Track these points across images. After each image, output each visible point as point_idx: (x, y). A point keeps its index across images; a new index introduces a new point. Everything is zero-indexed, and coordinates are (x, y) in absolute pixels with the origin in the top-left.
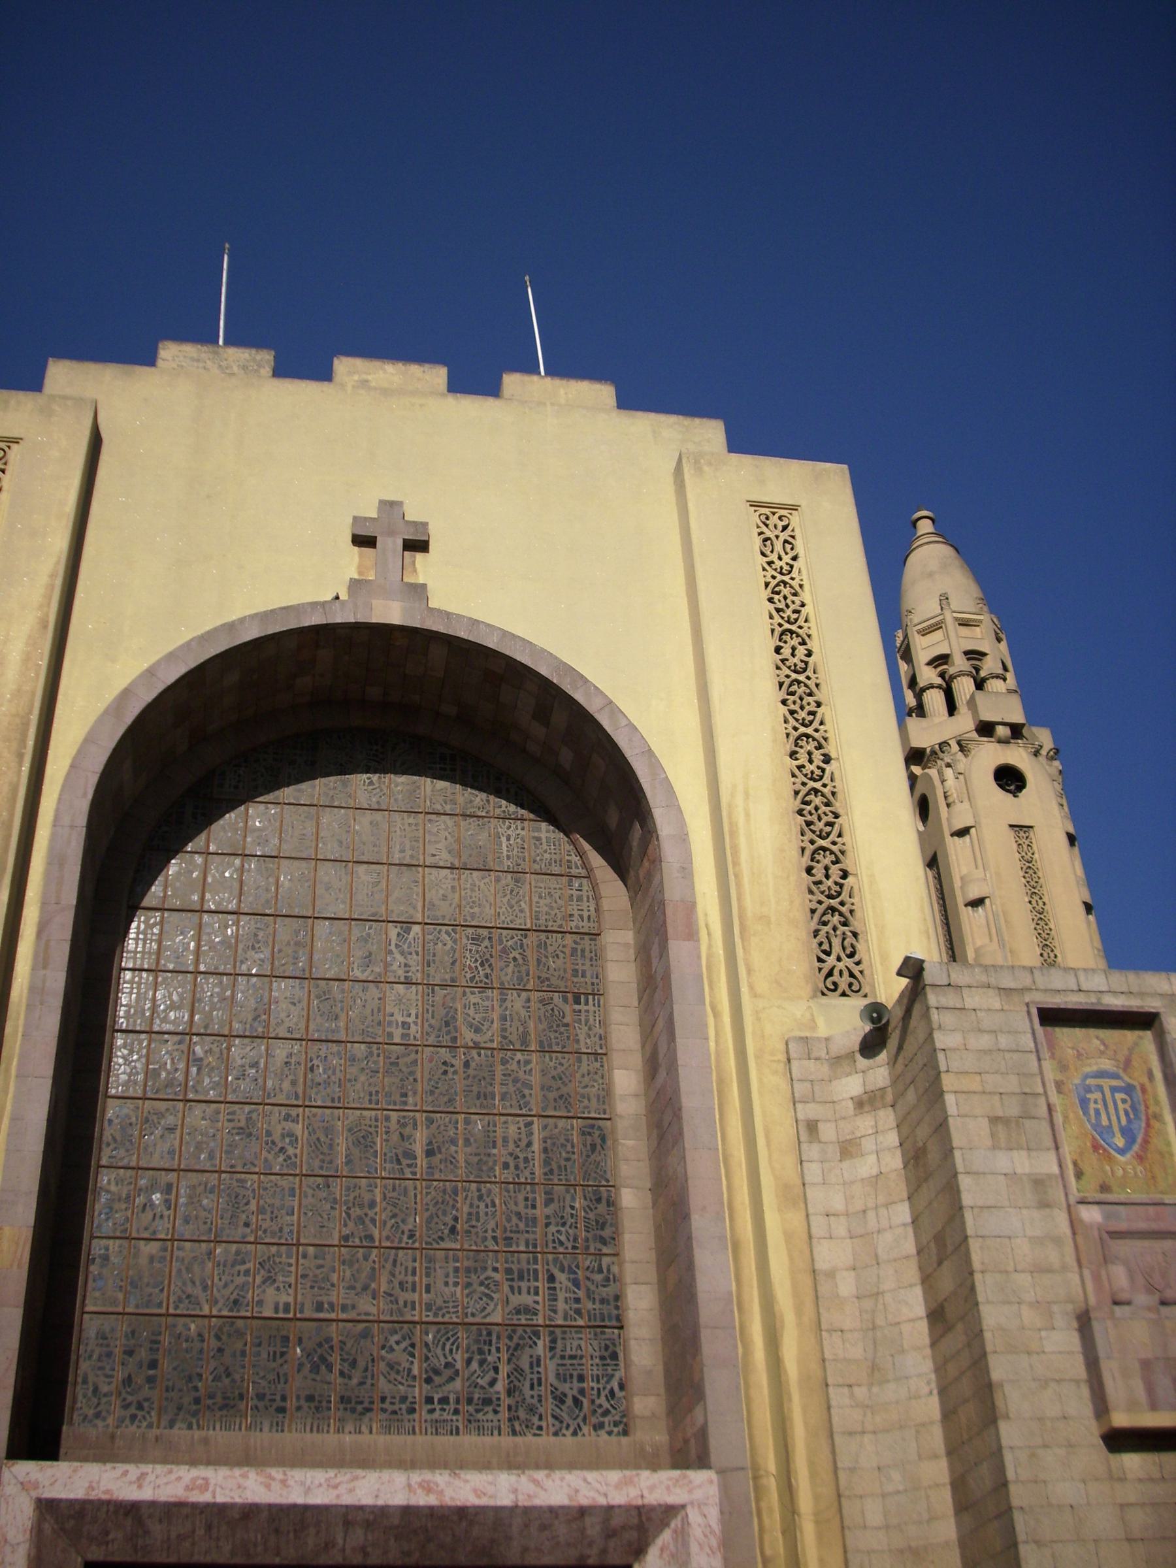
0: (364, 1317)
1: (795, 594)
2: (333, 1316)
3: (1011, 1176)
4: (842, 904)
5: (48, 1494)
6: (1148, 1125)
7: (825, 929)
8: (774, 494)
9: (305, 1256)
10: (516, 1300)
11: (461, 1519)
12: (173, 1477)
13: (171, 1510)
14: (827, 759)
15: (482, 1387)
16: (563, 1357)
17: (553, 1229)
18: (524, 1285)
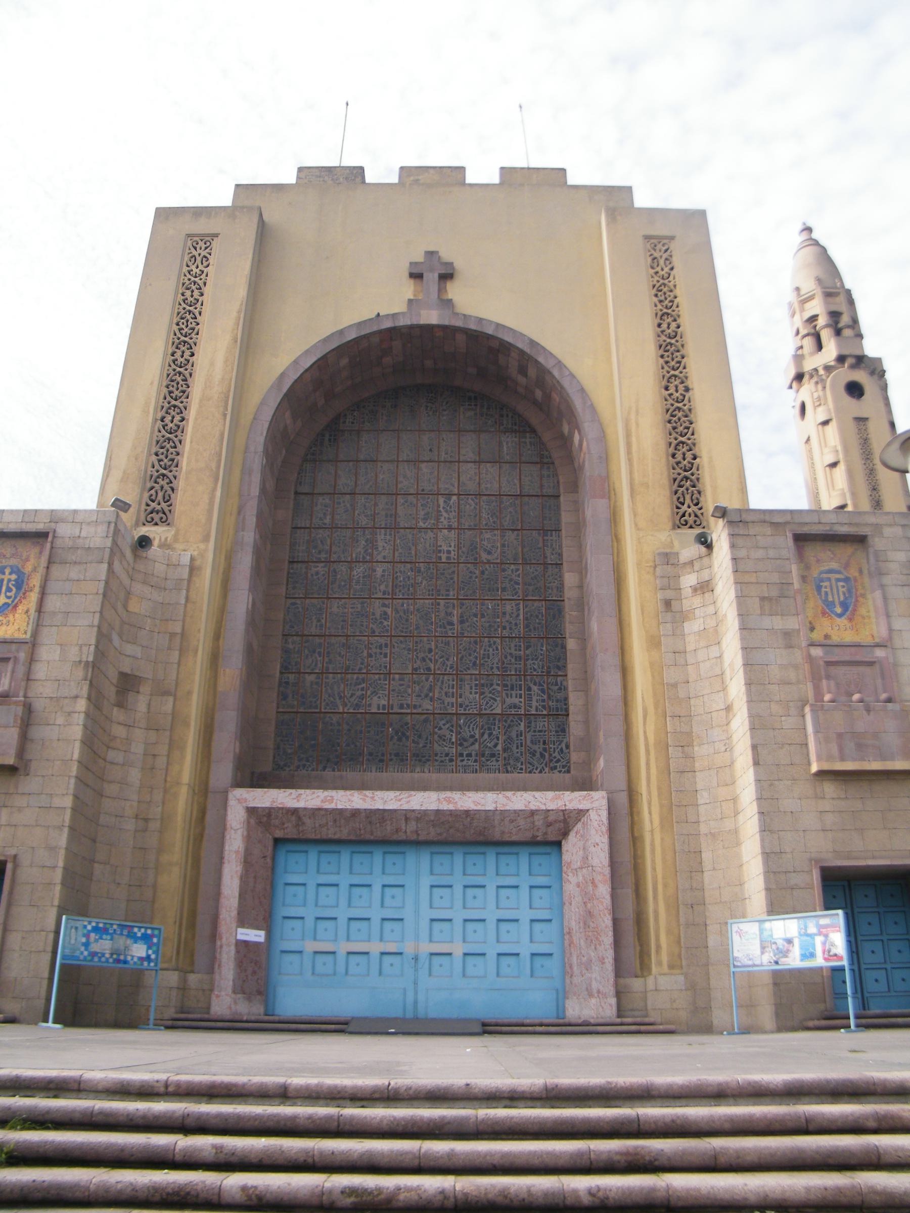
0: (425, 712)
1: (671, 291)
2: (409, 711)
3: (771, 631)
4: (693, 474)
5: (252, 805)
6: (857, 601)
7: (681, 489)
9: (394, 679)
10: (509, 701)
11: (467, 817)
12: (315, 796)
14: (687, 389)
15: (490, 748)
16: (535, 731)
17: (530, 662)
18: (514, 693)
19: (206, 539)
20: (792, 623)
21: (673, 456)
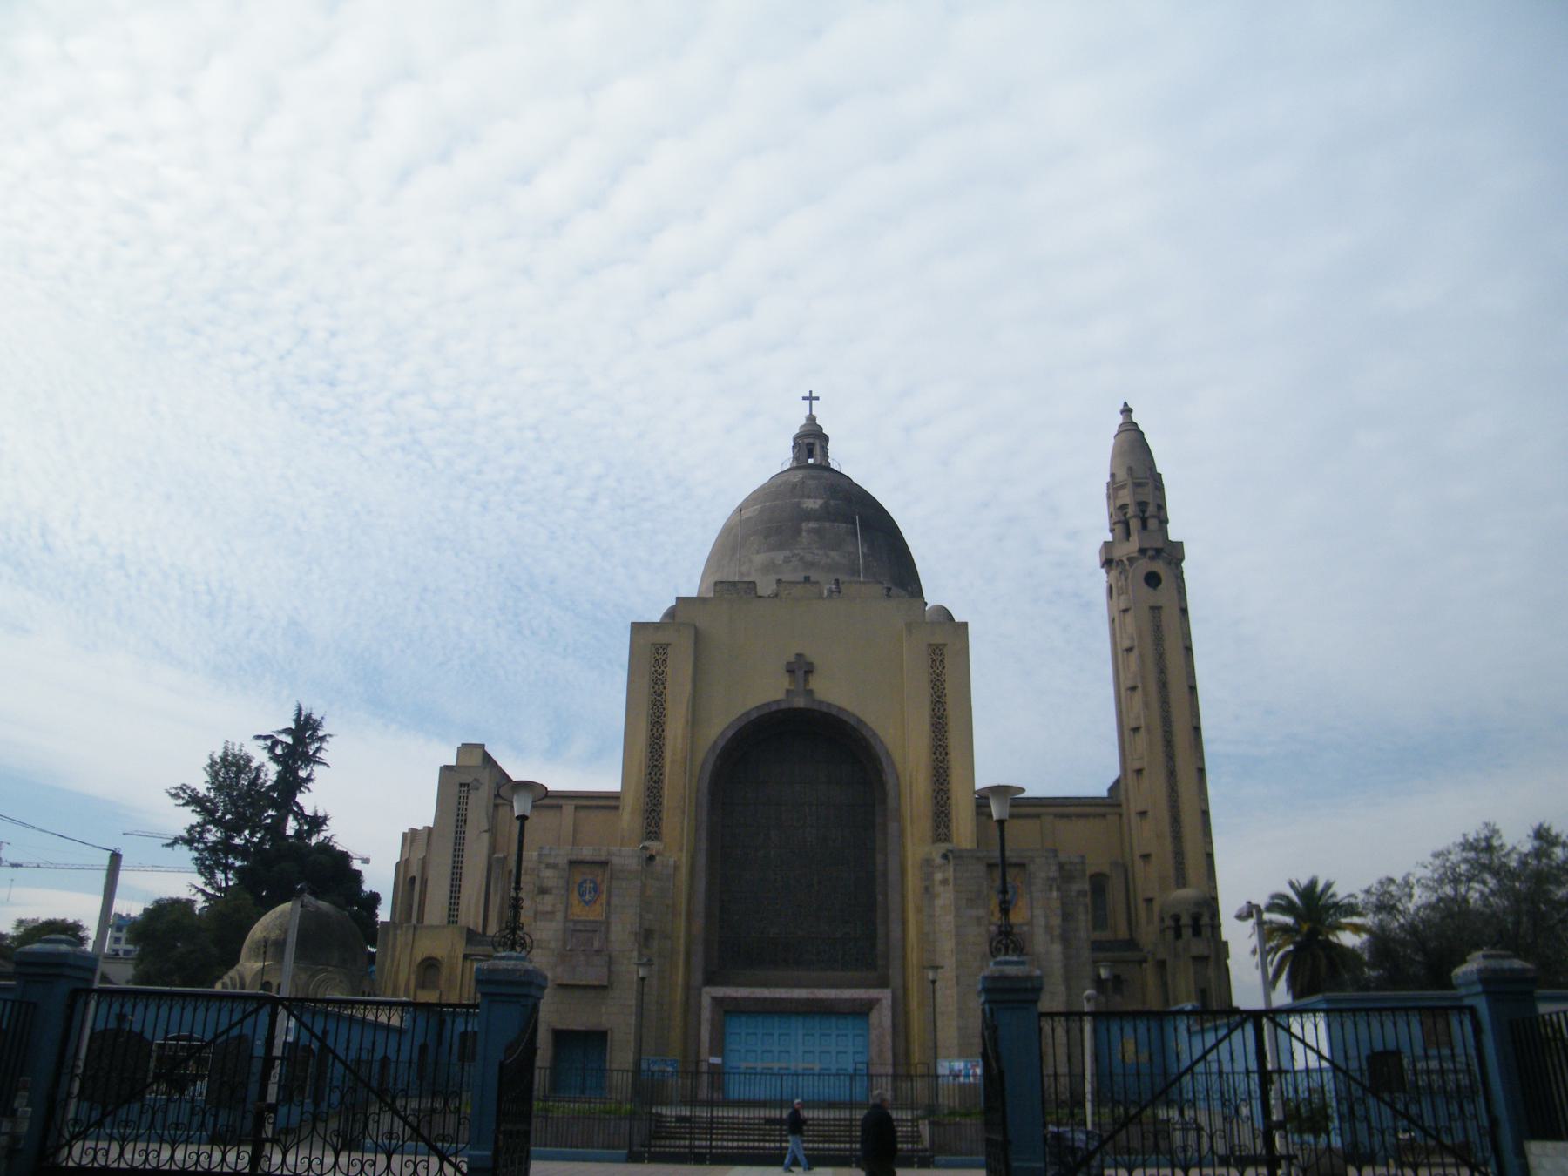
8: (938, 640)
13: (745, 999)
19: (681, 850)
20: (981, 912)
21: (936, 798)
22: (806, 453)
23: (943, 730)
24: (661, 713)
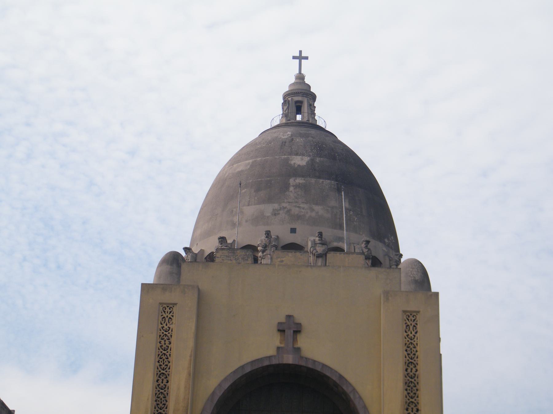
1: (415, 347)
22: (294, 110)
23: (415, 388)
24: (167, 365)
